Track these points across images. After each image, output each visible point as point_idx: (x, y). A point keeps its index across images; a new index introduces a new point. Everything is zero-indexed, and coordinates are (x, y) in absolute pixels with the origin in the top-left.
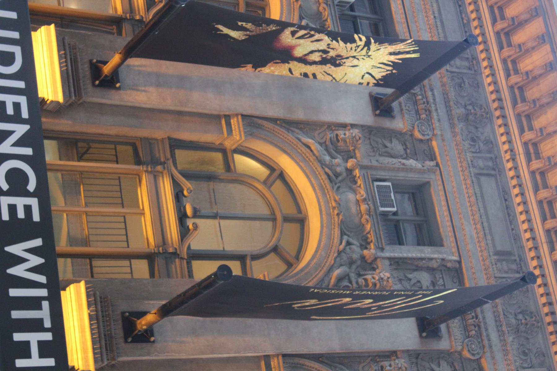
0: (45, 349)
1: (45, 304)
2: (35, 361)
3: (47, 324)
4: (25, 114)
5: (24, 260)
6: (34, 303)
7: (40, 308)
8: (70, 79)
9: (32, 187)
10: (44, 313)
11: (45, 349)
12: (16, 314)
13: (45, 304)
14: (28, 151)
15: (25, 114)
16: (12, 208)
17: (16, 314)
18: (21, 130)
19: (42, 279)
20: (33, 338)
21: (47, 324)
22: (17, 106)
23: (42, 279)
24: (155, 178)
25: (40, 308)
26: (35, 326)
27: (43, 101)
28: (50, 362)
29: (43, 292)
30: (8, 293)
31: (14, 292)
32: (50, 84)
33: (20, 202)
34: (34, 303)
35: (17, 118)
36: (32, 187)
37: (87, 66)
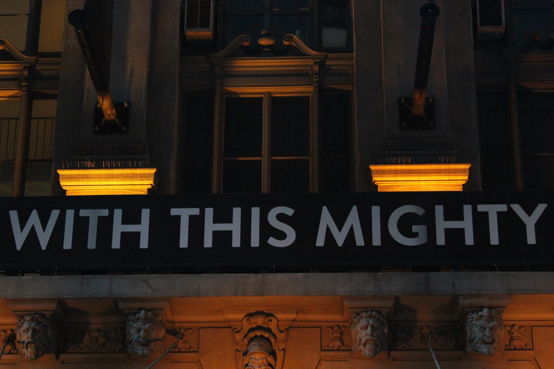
0: (132, 217)
1: (83, 213)
2: (143, 228)
3: (105, 212)
5: (33, 230)
6: (81, 225)
7: (86, 219)
10: (92, 215)
11: (132, 217)
12: (92, 244)
17: (92, 244)
19: (55, 214)
20: (119, 228)
21: (105, 212)
23: (55, 214)
25: (87, 219)
26: (105, 225)
28: (146, 213)
29: (70, 214)
30: (115, 250)
31: (68, 244)
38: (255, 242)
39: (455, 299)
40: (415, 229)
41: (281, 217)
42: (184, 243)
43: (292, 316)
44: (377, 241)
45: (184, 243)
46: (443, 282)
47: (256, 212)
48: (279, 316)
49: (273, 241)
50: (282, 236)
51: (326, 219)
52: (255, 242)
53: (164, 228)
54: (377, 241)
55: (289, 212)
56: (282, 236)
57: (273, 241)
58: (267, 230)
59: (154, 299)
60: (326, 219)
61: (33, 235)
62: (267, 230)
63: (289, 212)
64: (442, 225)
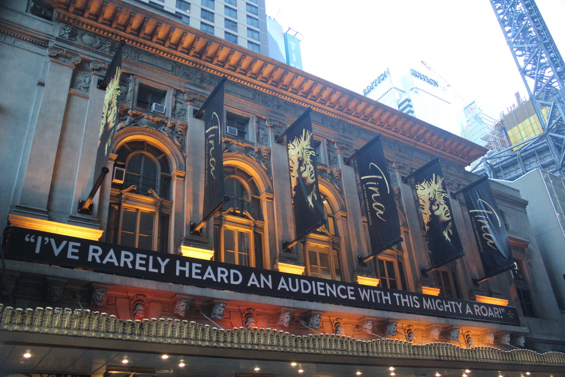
4: (323, 284)
8: (295, 261)
9: (345, 288)
13: (375, 291)
14: (334, 286)
15: (323, 284)
16: (352, 295)
18: (328, 287)
21: (380, 292)
22: (321, 286)
24: (308, 238)
27: (378, 285)
31: (374, 301)
32: (298, 270)
33: (350, 293)
34: (375, 294)
35: (325, 287)
36: (345, 288)
37: (285, 253)
38: (412, 306)
39: (452, 326)
40: (441, 306)
41: (416, 299)
42: (398, 304)
43: (416, 327)
44: (435, 309)
45: (398, 304)
46: (451, 321)
47: (410, 296)
48: (414, 327)
49: (415, 306)
50: (417, 305)
51: (424, 302)
52: (412, 306)
53: (393, 298)
54: (435, 309)
55: (417, 298)
56: (417, 305)
57: (415, 306)
58: (414, 303)
59: (397, 320)
60: (424, 302)
61: (365, 297)
62: (414, 303)
63: (417, 298)
64: (445, 306)
